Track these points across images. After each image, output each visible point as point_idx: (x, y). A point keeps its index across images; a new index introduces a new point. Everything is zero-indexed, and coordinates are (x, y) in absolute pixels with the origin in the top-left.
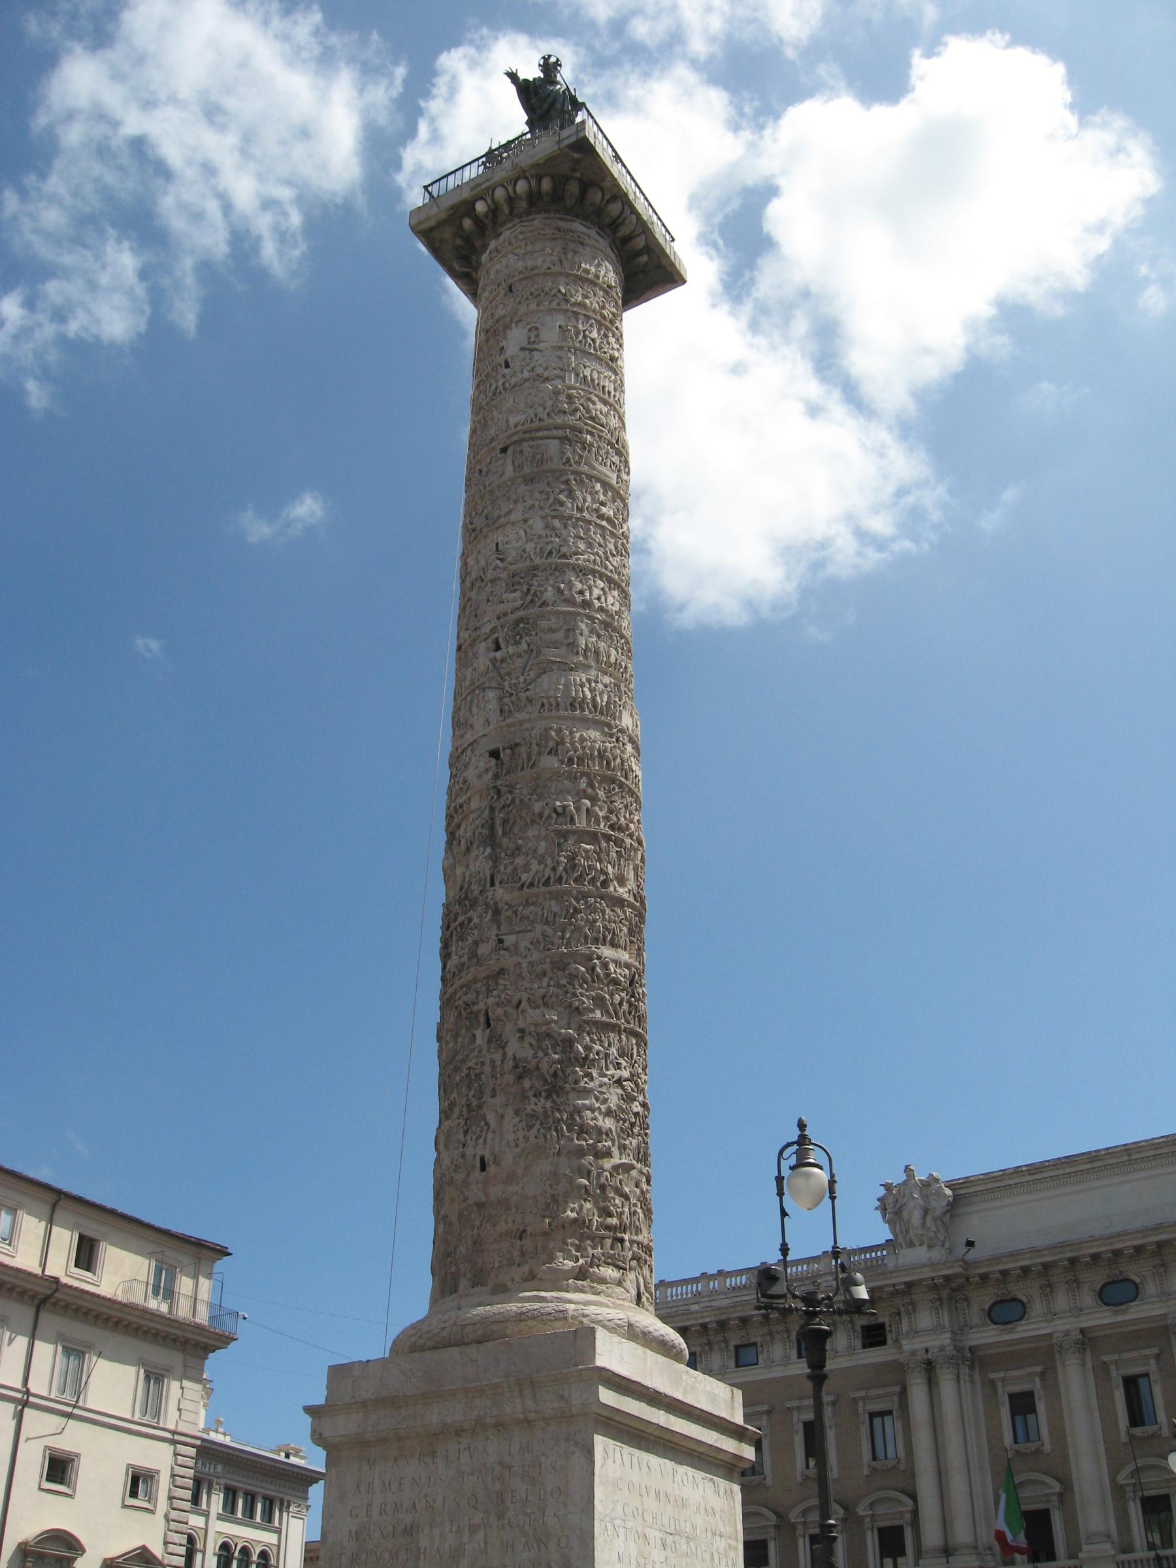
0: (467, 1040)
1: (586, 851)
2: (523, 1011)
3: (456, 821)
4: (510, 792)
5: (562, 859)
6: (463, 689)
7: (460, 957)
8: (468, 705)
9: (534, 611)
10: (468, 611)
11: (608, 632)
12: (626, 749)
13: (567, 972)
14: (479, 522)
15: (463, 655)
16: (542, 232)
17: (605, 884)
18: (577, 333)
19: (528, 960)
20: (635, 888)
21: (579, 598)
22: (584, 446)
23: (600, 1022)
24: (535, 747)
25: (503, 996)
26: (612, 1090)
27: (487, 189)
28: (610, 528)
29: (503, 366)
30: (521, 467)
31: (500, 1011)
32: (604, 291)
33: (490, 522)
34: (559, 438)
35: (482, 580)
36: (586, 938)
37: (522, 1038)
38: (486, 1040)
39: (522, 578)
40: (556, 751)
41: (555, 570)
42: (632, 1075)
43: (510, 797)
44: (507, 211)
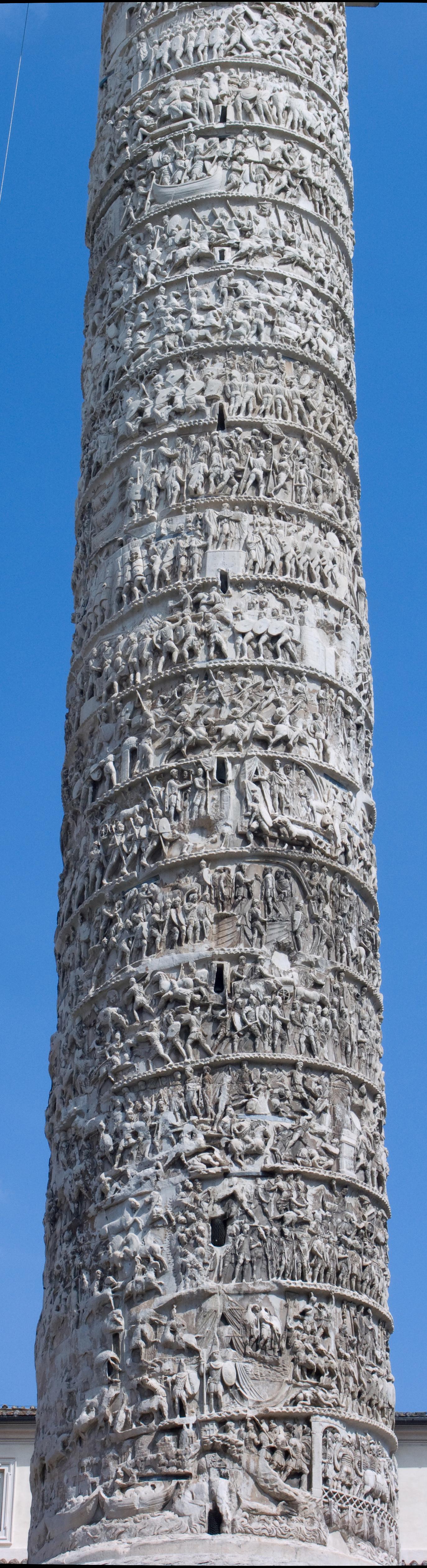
17: (157, 854)
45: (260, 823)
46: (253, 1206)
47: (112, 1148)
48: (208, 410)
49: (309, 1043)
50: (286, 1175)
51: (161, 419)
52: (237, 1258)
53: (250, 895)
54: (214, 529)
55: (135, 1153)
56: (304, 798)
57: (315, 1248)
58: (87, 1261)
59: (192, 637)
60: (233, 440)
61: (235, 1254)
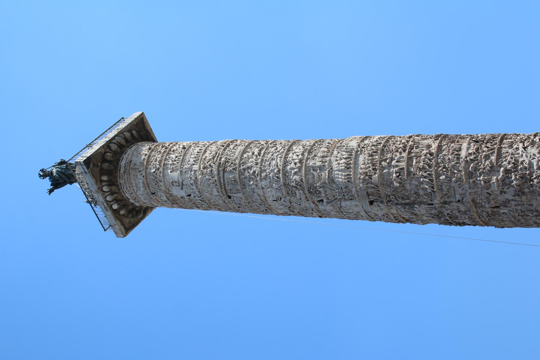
0: (505, 216)
1: (416, 163)
2: (492, 192)
3: (401, 219)
4: (389, 196)
5: (420, 174)
6: (340, 215)
7: (465, 218)
8: (348, 214)
9: (305, 185)
10: (304, 213)
11: (313, 151)
12: (367, 144)
13: (473, 172)
14: (263, 208)
15: (324, 215)
16: (126, 179)
17: (431, 154)
18: (174, 164)
19: (468, 189)
20: (431, 140)
21: (298, 165)
22: (226, 162)
23: (497, 157)
24: (368, 186)
25: (485, 200)
26: (529, 152)
27: (107, 204)
28: (264, 150)
29: (190, 197)
30: (238, 190)
31: (492, 202)
32: (152, 152)
33: (263, 203)
34: (224, 173)
35: (290, 207)
36: (457, 163)
37: (505, 192)
38: (505, 208)
39: (289, 190)
40: (370, 176)
41: (285, 175)
42: (521, 142)
43: (391, 197)
44: (117, 195)
47: (513, 165)
51: (302, 158)
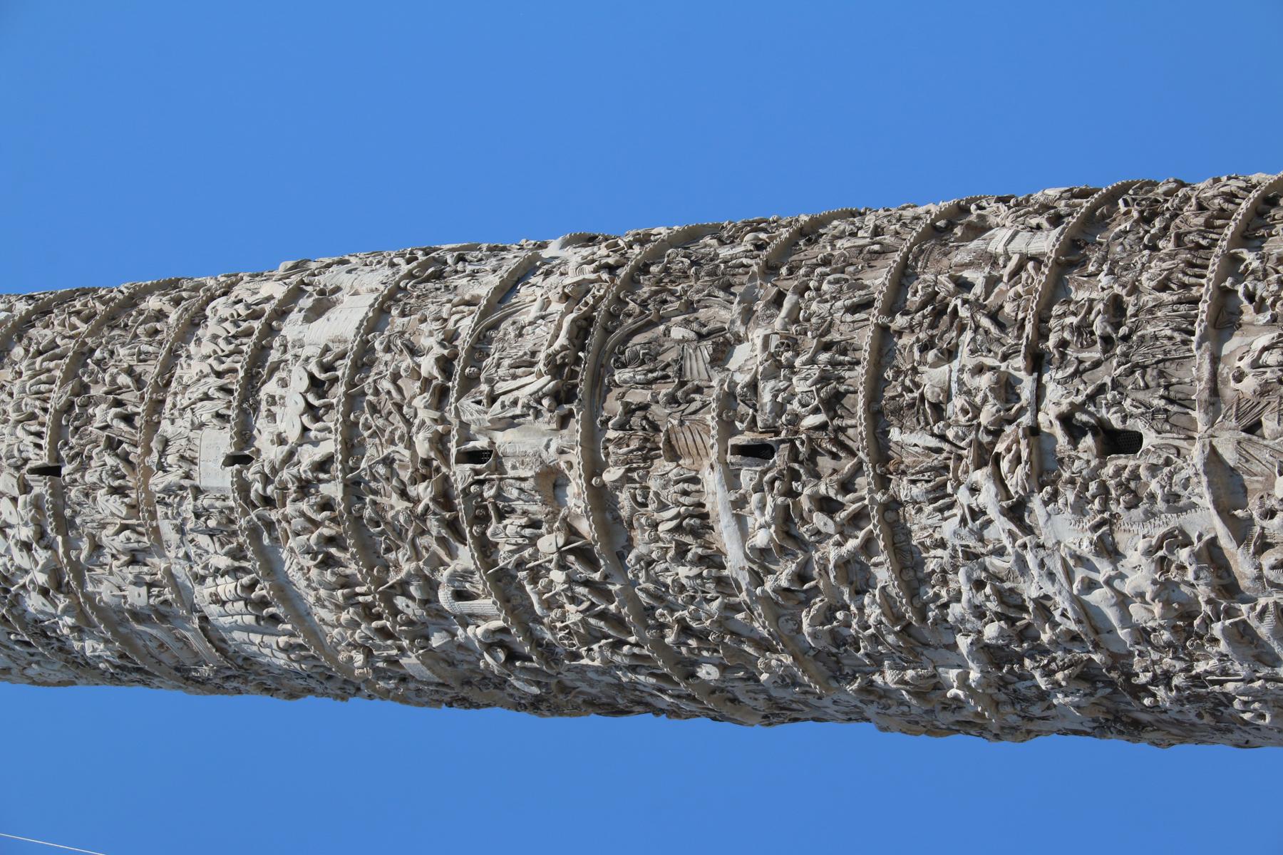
45: (545, 395)
46: (1081, 387)
48: (36, 490)
49: (853, 309)
50: (1042, 334)
51: (48, 560)
52: (1158, 411)
53: (644, 407)
54: (173, 477)
55: (1007, 585)
56: (524, 331)
57: (1153, 284)
58: (1179, 665)
59: (304, 506)
60: (73, 452)
61: (1152, 414)
